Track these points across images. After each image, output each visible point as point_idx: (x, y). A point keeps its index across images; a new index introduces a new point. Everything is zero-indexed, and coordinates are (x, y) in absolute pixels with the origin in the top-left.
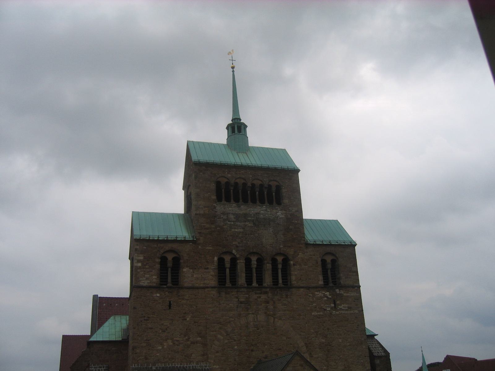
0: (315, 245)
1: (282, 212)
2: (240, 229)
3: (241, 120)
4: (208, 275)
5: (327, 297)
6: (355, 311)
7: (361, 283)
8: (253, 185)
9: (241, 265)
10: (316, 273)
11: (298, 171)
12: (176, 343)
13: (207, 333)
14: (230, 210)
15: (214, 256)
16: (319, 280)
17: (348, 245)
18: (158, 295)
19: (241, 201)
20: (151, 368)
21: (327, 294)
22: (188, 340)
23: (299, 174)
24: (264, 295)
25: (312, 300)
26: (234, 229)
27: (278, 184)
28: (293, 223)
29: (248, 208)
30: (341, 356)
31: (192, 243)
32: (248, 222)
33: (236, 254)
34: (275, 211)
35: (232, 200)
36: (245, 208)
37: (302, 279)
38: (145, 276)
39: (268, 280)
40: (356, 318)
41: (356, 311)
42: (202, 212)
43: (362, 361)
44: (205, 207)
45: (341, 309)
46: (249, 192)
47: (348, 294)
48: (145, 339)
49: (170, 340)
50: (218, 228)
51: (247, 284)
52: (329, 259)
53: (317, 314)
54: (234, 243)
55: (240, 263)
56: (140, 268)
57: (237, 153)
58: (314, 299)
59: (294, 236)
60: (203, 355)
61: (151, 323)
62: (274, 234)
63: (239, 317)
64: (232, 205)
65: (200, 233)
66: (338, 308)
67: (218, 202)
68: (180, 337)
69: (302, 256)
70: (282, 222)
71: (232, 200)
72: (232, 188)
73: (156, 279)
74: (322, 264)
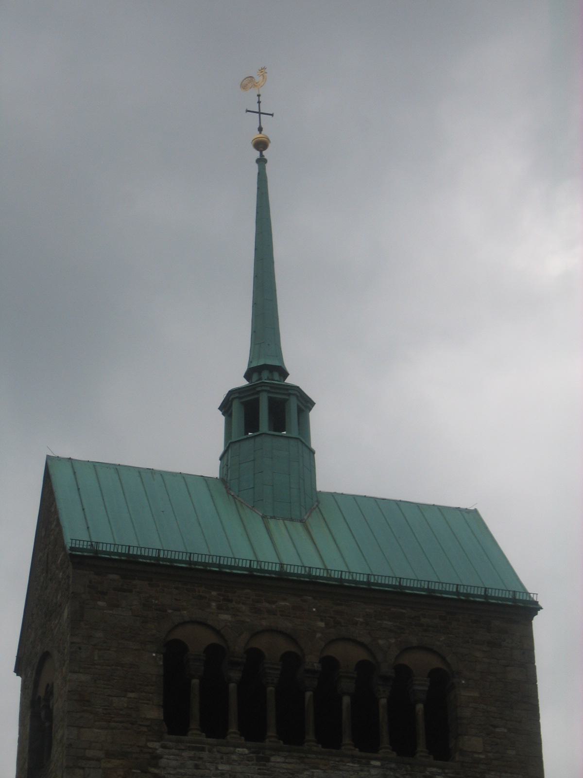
3: (284, 374)
8: (329, 664)
11: (530, 608)
19: (272, 732)
23: (533, 621)
35: (233, 729)
36: (289, 766)
46: (308, 694)
57: (264, 517)
64: (233, 753)
71: (233, 729)
72: (236, 675)
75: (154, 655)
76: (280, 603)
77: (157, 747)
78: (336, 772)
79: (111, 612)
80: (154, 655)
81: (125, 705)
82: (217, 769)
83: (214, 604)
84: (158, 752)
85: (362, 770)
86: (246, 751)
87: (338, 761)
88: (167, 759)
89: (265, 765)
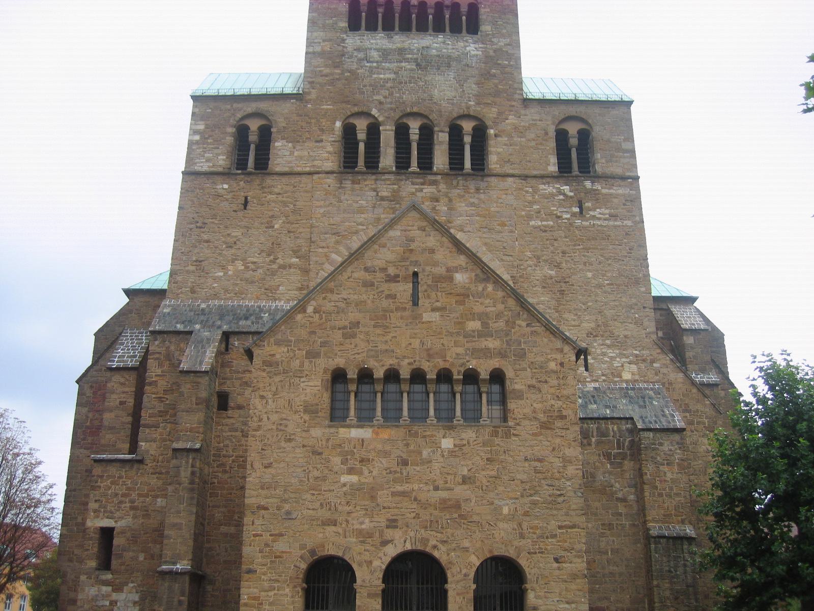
0: (543, 102)
1: (477, 46)
2: (390, 73)
4: (321, 152)
5: (564, 194)
6: (625, 222)
7: (641, 171)
9: (387, 135)
10: (542, 152)
12: (252, 266)
13: (311, 250)
15: (335, 121)
16: (549, 165)
17: (615, 101)
18: (226, 186)
20: (199, 305)
21: (564, 190)
22: (273, 261)
24: (429, 187)
25: (530, 198)
26: (377, 74)
28: (499, 64)
30: (590, 304)
33: (379, 116)
37: (511, 160)
38: (204, 156)
39: (441, 159)
40: (627, 234)
41: (629, 223)
42: (318, 49)
43: (637, 316)
44: (324, 41)
45: (594, 217)
46: (414, 16)
47: (612, 191)
48: (194, 259)
49: (239, 262)
50: (347, 74)
51: (397, 167)
52: (573, 129)
53: (540, 223)
55: (386, 130)
56: (197, 142)
58: (537, 197)
59: (501, 87)
60: (301, 289)
61: (209, 232)
63: (376, 224)
66: (589, 216)
68: (258, 257)
69: (514, 121)
70: (477, 62)
73: (223, 160)
74: (556, 136)
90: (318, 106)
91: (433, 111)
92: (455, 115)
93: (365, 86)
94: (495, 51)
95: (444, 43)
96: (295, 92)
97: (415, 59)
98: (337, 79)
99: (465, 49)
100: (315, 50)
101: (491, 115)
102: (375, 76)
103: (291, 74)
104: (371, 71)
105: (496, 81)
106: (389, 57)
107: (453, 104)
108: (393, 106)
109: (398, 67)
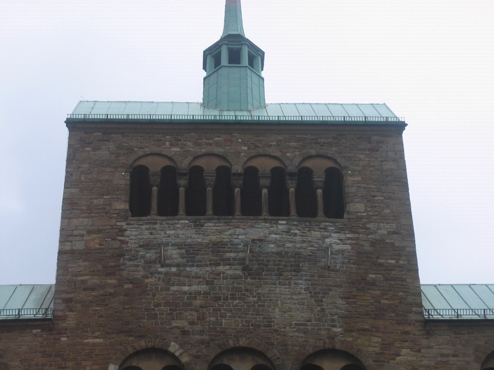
1: (342, 236)
2: (199, 283)
11: (400, 126)
14: (169, 236)
23: (403, 135)
26: (178, 285)
27: (331, 164)
28: (381, 265)
29: (230, 229)
31: (39, 330)
32: (224, 265)
33: (181, 354)
34: (316, 233)
42: (79, 245)
44: (89, 232)
46: (237, 190)
50: (126, 286)
54: (174, 324)
59: (386, 302)
62: (310, 296)
64: (177, 224)
65: (69, 300)
67: (130, 218)
69: (410, 358)
70: (343, 263)
72: (183, 182)
75: (123, 173)
76: (216, 139)
77: (124, 225)
78: (253, 229)
79: (95, 153)
80: (123, 173)
81: (102, 203)
82: (165, 233)
83: (167, 143)
84: (124, 227)
85: (272, 227)
86: (187, 222)
87: (254, 223)
88: (130, 231)
89: (200, 229)
90: (78, 340)
91: (272, 344)
92: (311, 350)
93: (158, 305)
94: (373, 244)
95: (288, 232)
96: (40, 316)
97: (240, 259)
98: (111, 294)
99: (323, 243)
100: (75, 248)
101: (371, 349)
102: (175, 288)
103: (33, 288)
104: (168, 280)
105: (378, 293)
106: (199, 257)
107: (305, 333)
108: (206, 337)
109: (212, 273)
